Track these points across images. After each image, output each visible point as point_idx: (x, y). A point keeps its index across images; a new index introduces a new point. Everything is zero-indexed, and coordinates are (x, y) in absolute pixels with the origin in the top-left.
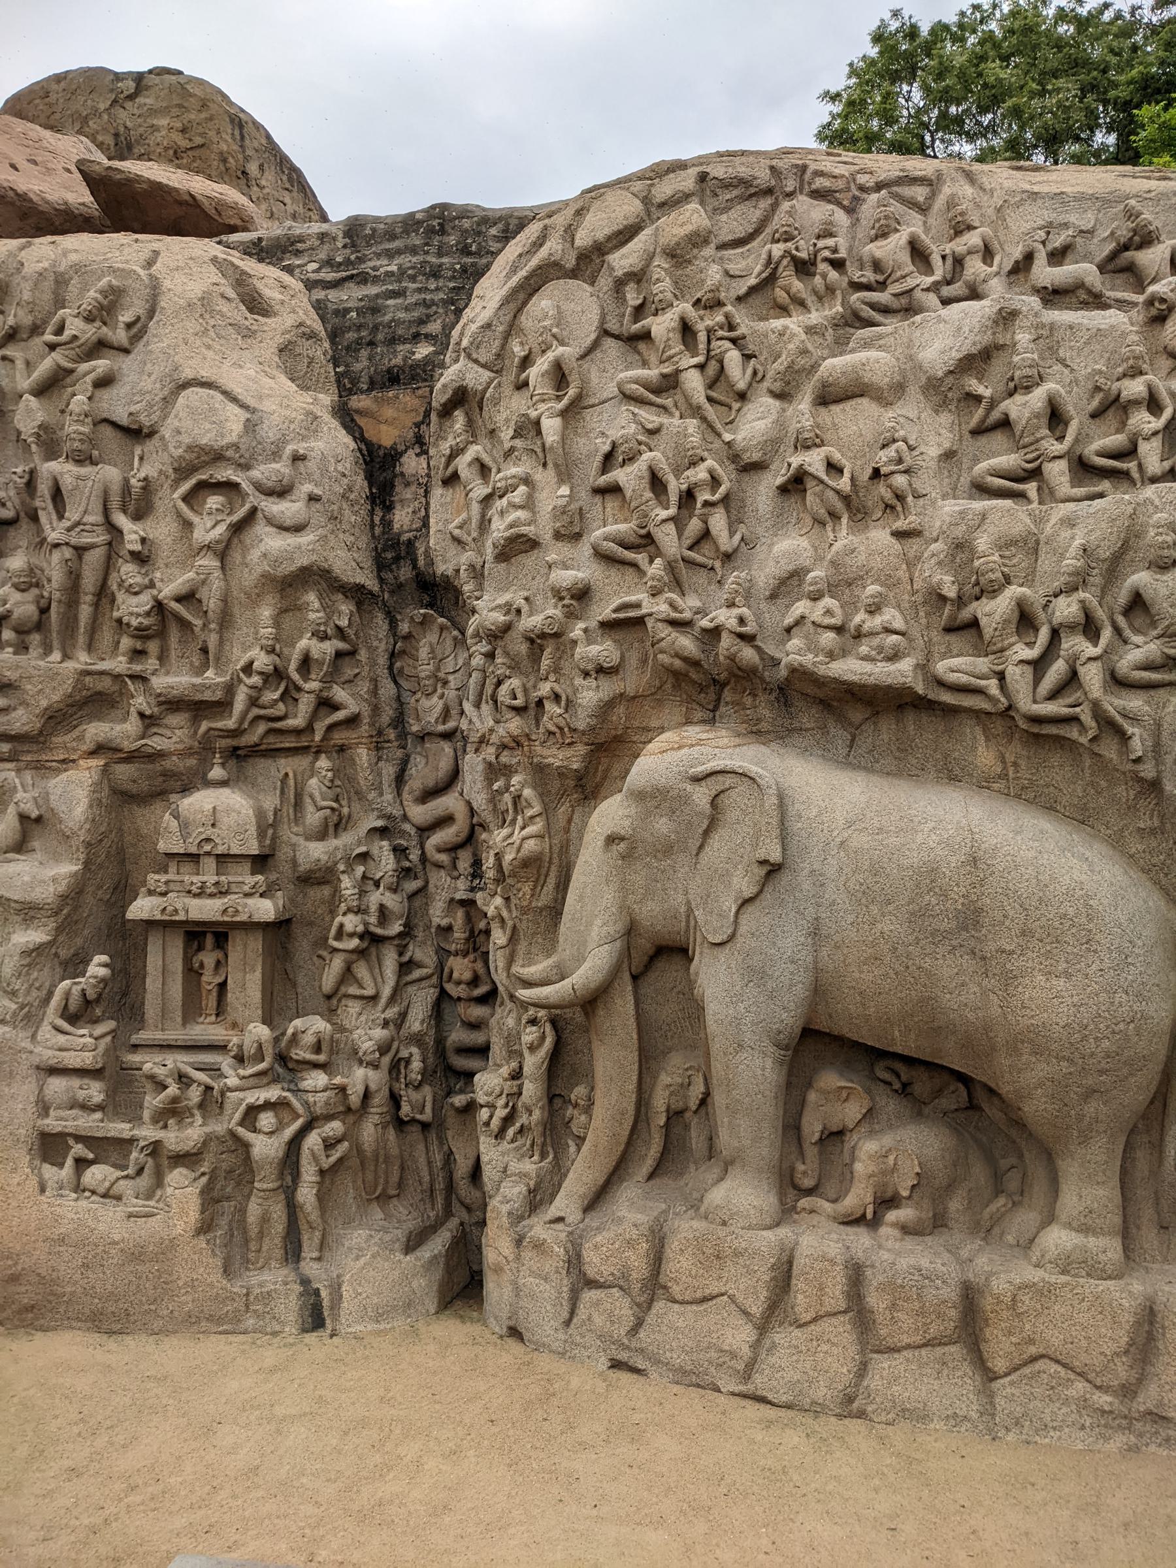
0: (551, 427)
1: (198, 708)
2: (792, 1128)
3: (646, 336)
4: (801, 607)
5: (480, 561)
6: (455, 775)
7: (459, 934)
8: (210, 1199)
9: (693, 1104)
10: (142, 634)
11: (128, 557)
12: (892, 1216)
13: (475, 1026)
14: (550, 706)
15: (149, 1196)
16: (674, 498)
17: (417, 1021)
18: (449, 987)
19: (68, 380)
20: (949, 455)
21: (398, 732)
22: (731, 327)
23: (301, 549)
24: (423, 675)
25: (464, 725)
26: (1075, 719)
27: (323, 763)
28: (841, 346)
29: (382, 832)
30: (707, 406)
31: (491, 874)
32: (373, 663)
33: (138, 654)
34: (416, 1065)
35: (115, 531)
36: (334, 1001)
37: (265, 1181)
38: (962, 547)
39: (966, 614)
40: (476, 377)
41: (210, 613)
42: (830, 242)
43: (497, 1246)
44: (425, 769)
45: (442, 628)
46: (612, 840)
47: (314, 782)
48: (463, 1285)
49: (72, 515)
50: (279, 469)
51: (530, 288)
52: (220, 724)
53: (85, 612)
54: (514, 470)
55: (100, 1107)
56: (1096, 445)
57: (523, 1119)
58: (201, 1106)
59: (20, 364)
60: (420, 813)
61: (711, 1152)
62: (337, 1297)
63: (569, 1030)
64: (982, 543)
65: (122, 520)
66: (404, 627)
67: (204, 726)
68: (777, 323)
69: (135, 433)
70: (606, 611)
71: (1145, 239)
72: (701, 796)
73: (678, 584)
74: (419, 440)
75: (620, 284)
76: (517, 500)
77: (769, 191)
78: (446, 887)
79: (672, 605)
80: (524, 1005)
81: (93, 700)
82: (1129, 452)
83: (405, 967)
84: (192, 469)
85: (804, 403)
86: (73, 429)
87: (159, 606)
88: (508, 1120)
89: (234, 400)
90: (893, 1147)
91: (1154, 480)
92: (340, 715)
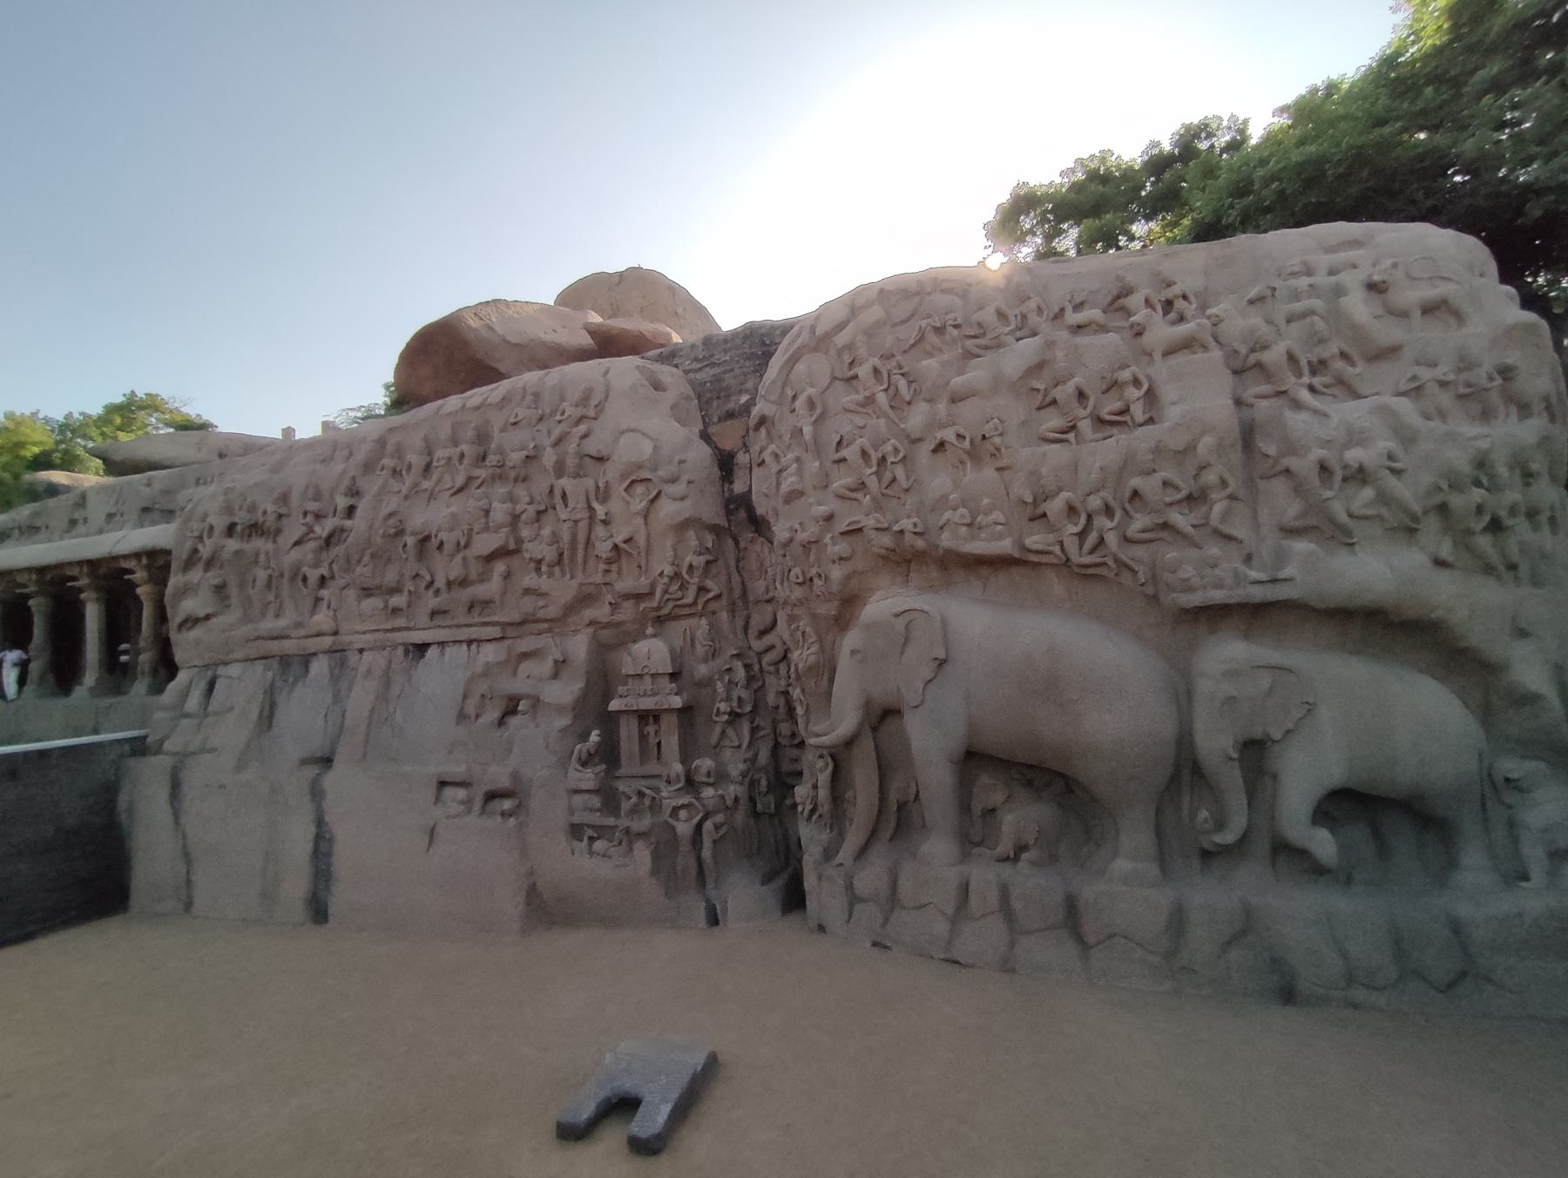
0: (807, 430)
1: (638, 597)
2: (965, 807)
3: (856, 377)
4: (947, 515)
6: (775, 623)
7: (782, 710)
8: (656, 856)
9: (912, 798)
10: (609, 562)
12: (1025, 856)
13: (796, 760)
14: (817, 582)
16: (874, 461)
17: (764, 757)
20: (1024, 423)
21: (741, 600)
22: (900, 367)
23: (685, 509)
26: (1105, 564)
27: (704, 621)
28: (961, 372)
29: (738, 656)
30: (890, 411)
32: (727, 565)
34: (764, 783)
35: (590, 508)
37: (685, 847)
38: (1034, 474)
39: (1040, 511)
42: (951, 316)
43: (810, 882)
44: (758, 620)
46: (853, 652)
48: (794, 899)
49: (571, 504)
50: (673, 468)
51: (794, 360)
53: (580, 553)
54: (789, 456)
55: (599, 810)
56: (1108, 408)
57: (820, 810)
58: (651, 807)
60: (757, 645)
61: (924, 826)
62: (725, 910)
63: (839, 757)
64: (1044, 470)
65: (596, 505)
66: (742, 545)
67: (642, 606)
68: (924, 363)
69: (600, 459)
70: (843, 527)
71: (1126, 292)
72: (900, 624)
73: (877, 506)
74: (745, 445)
75: (840, 352)
77: (917, 294)
78: (774, 685)
79: (878, 521)
80: (817, 747)
81: (586, 598)
82: (1125, 411)
83: (754, 730)
84: (629, 474)
85: (942, 407)
86: (571, 462)
87: (616, 547)
88: (813, 811)
89: (645, 435)
90: (1022, 817)
91: (1141, 425)
92: (710, 595)
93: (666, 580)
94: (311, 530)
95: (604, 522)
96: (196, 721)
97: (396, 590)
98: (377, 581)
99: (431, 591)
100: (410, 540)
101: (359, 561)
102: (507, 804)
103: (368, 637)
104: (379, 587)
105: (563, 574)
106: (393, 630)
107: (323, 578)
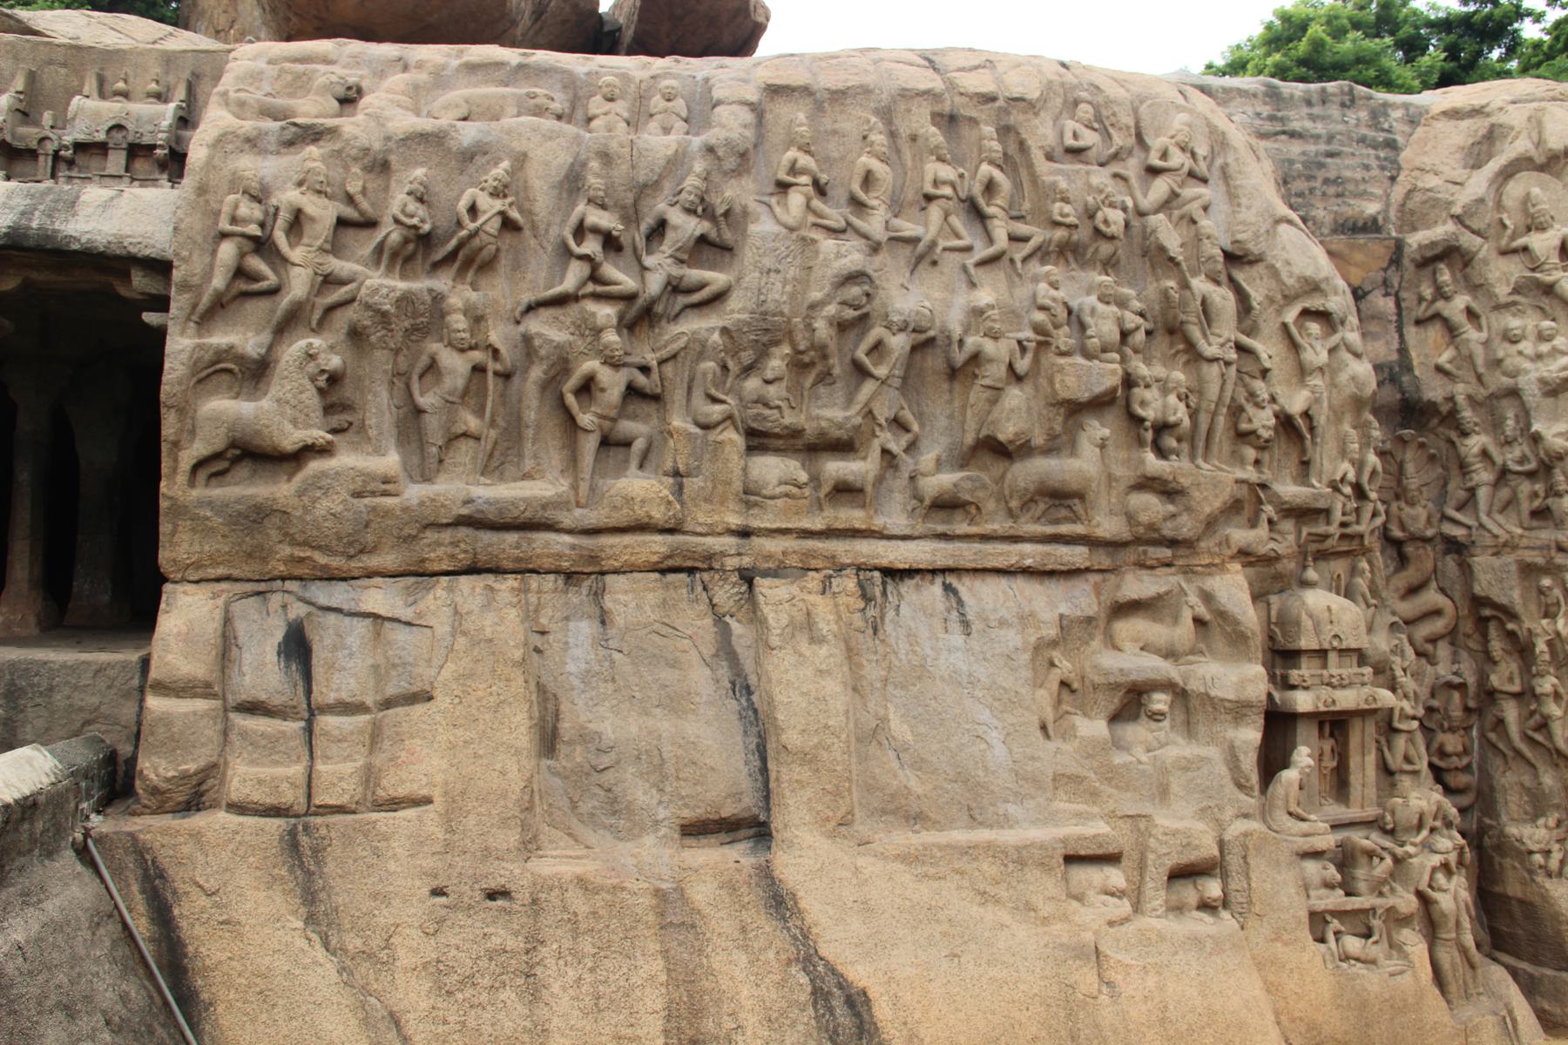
1: (1302, 514)
5: (1482, 393)
7: (1457, 713)
11: (1258, 374)
15: (1389, 957)
18: (1436, 760)
19: (1175, 203)
24: (1413, 487)
25: (1458, 532)
31: (1547, 657)
33: (1257, 462)
36: (1397, 777)
40: (1468, 240)
41: (1319, 430)
45: (1422, 446)
47: (1359, 581)
52: (1321, 529)
53: (1221, 419)
59: (1134, 181)
60: (1408, 608)
69: (1234, 258)
76: (1563, 348)
93: (1348, 490)
94: (594, 277)
95: (1265, 372)
96: (294, 726)
97: (844, 447)
98: (789, 419)
99: (927, 458)
100: (899, 343)
101: (748, 370)
102: (1213, 888)
103: (774, 546)
104: (796, 433)
105: (1193, 458)
106: (829, 533)
107: (632, 391)
